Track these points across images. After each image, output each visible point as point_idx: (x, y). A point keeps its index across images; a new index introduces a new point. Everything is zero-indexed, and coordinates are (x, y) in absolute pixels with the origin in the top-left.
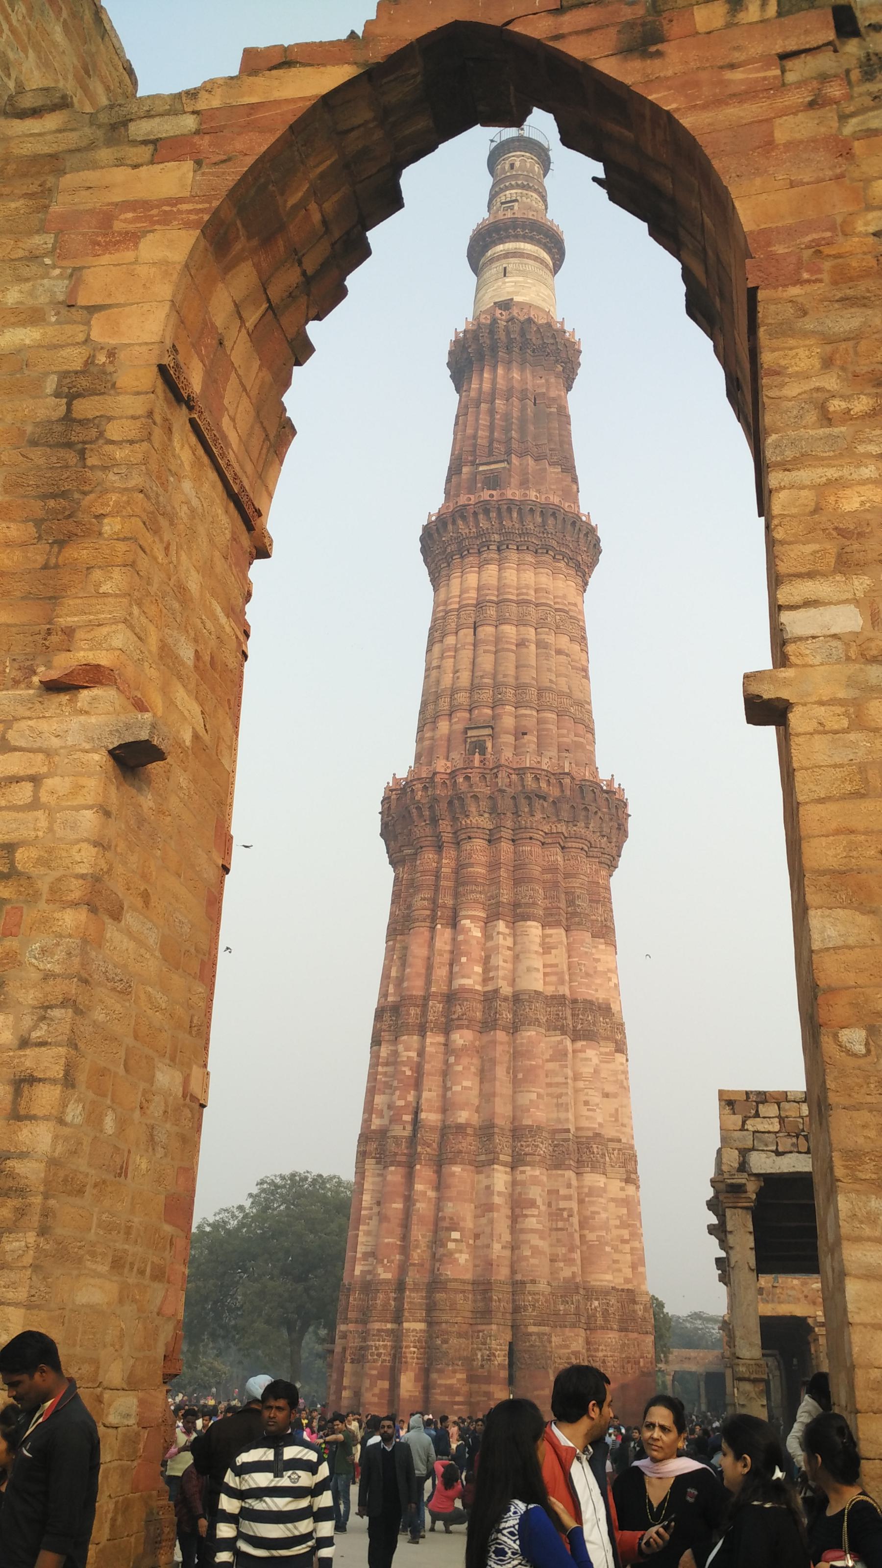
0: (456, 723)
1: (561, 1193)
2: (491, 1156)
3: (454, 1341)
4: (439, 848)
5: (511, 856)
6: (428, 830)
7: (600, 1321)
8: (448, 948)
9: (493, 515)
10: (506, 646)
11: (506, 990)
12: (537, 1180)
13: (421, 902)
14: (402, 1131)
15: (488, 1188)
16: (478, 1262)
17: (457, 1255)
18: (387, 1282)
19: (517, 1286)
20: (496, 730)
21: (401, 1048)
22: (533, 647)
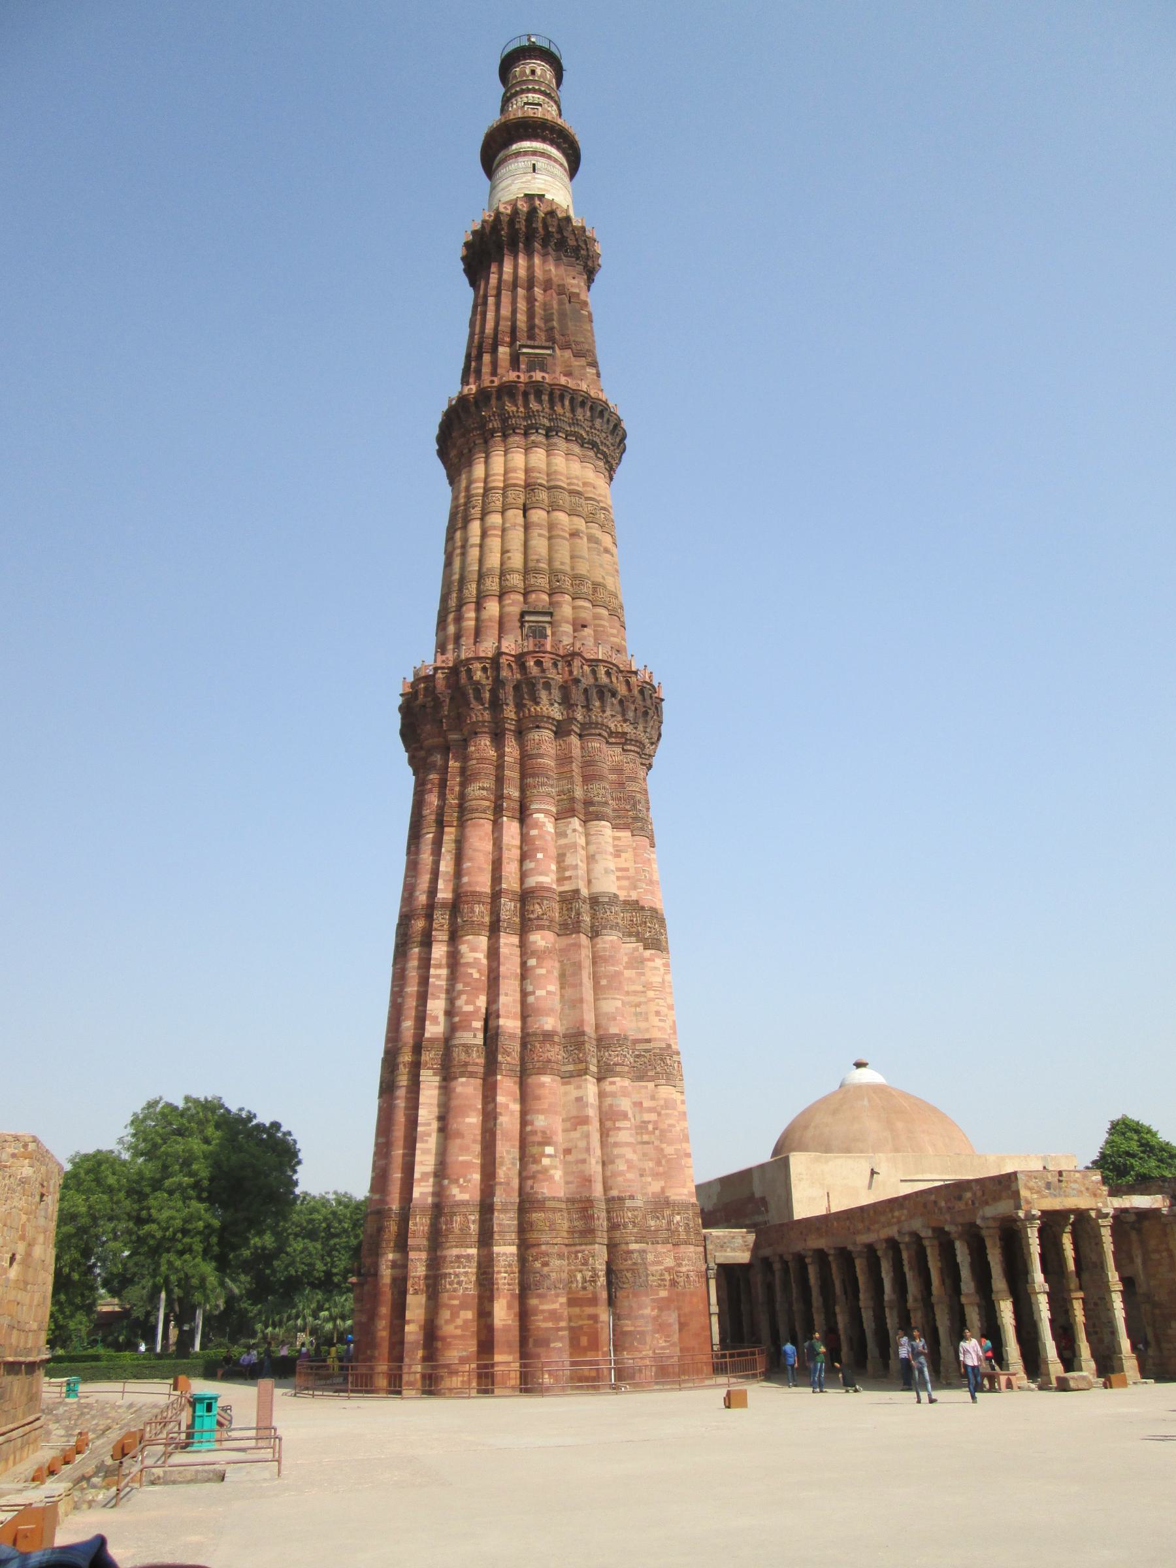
0: (510, 605)
1: (645, 1105)
3: (555, 1263)
4: (498, 738)
5: (578, 750)
6: (487, 716)
7: (683, 1236)
8: (517, 842)
9: (545, 398)
10: (562, 533)
11: (584, 892)
14: (473, 1037)
15: (579, 1099)
16: (571, 1179)
17: (552, 1172)
19: (614, 1203)
20: (557, 617)
21: (464, 948)
22: (585, 539)
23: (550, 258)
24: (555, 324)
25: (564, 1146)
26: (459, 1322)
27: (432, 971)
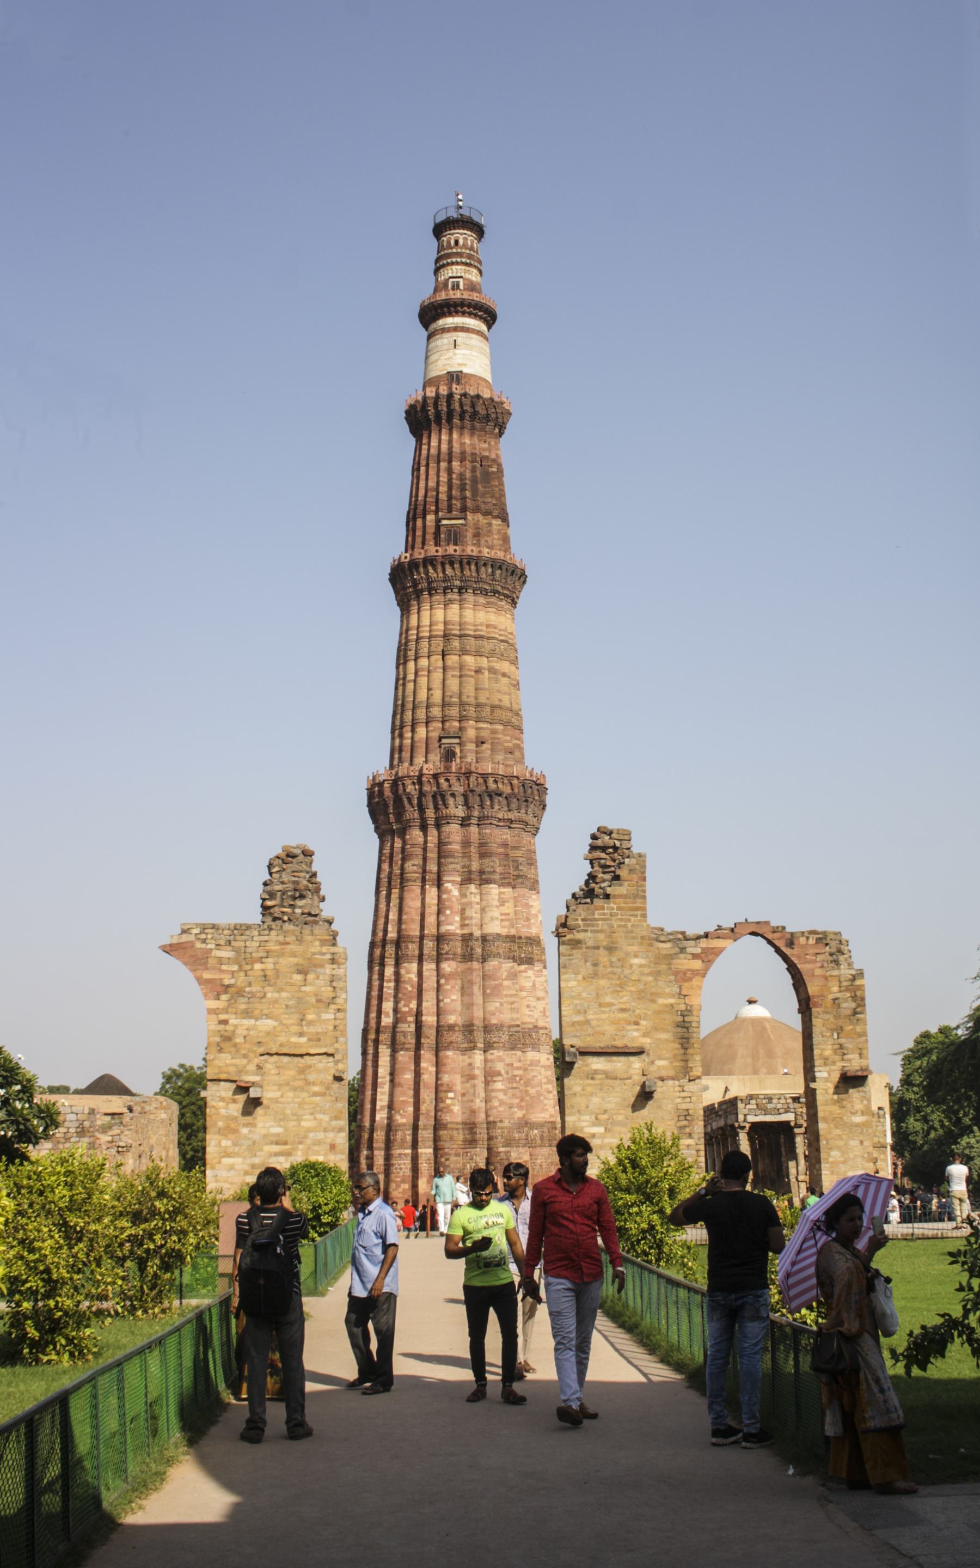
2: (472, 1045)
3: (453, 1158)
4: (424, 828)
5: (477, 835)
6: (416, 815)
8: (436, 902)
9: (457, 566)
10: (468, 673)
11: (477, 933)
12: (501, 1058)
13: (413, 867)
15: (470, 1064)
18: (404, 1125)
19: (490, 1125)
20: (463, 739)
21: (403, 971)
22: (486, 673)
23: (466, 431)
24: (468, 494)
25: (463, 1091)
26: (401, 1190)
27: (385, 984)
